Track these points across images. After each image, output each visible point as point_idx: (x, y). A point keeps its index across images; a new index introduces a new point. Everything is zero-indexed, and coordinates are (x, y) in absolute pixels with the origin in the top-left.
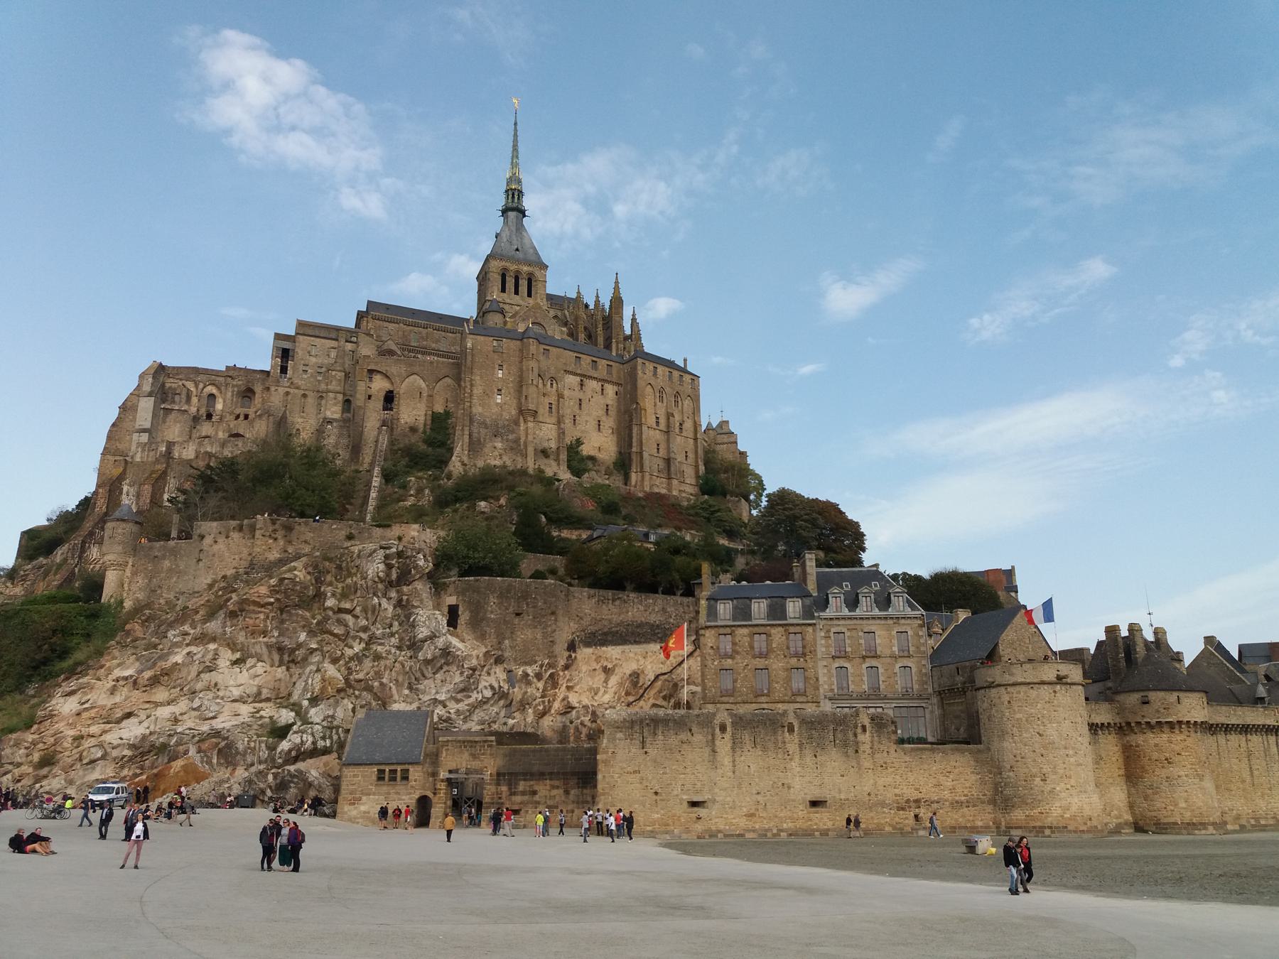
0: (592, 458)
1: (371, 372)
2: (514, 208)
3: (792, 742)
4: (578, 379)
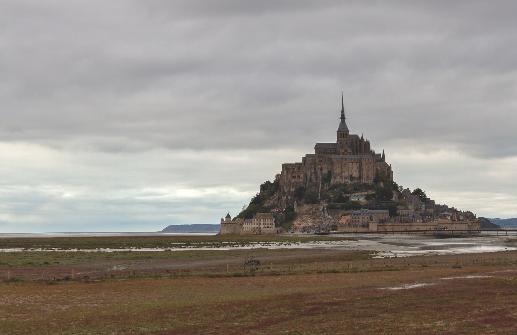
0: (355, 177)
1: (318, 164)
2: (343, 118)
3: (352, 227)
4: (352, 163)
